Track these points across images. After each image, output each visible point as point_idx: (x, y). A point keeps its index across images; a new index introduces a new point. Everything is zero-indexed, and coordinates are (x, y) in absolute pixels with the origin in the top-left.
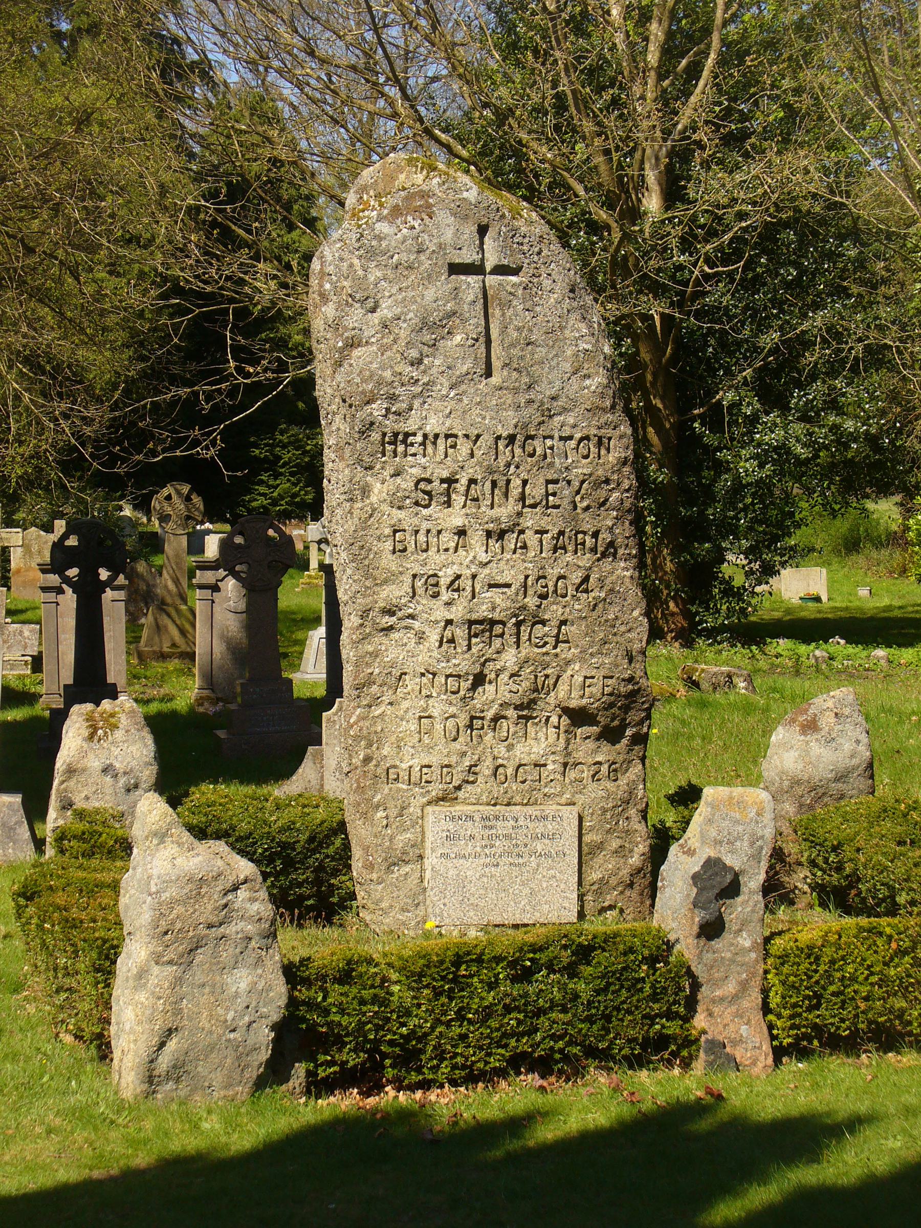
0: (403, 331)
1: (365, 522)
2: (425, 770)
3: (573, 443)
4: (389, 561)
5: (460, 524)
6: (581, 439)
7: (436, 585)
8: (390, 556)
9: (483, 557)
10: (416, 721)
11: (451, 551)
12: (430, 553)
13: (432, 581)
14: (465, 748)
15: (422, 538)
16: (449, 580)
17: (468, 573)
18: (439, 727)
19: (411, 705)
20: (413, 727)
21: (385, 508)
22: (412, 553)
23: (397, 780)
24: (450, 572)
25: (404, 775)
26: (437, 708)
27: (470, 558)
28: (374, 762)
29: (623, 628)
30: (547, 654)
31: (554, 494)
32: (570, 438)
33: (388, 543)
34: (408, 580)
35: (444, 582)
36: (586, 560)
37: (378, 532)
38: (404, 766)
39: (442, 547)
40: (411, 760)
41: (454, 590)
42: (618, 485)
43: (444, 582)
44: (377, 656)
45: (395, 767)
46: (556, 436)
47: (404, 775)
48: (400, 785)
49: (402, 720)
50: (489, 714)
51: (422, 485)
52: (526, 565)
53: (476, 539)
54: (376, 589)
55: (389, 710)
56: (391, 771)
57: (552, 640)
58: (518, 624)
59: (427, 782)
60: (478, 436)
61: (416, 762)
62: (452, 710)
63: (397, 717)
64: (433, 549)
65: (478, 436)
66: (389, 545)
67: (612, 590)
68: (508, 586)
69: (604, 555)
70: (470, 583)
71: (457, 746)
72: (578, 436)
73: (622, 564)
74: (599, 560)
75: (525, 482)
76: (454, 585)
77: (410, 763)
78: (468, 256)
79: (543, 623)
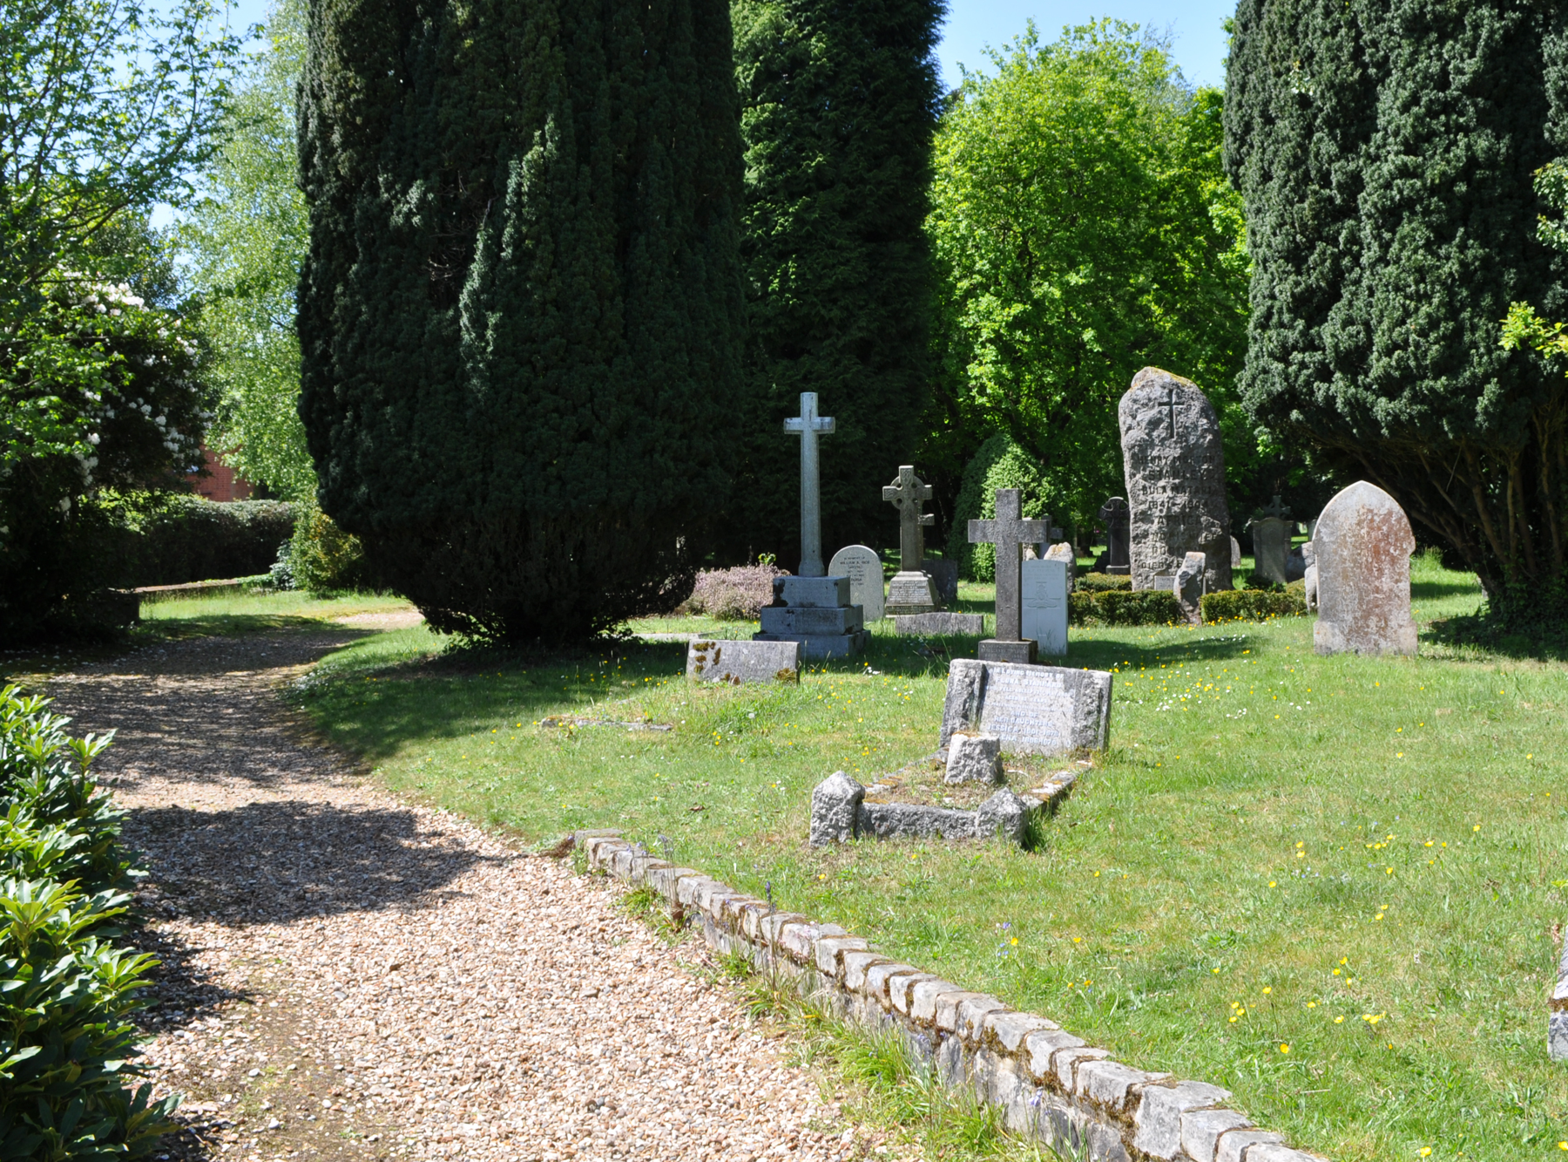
0: (1144, 425)
4: (1142, 498)
40: (1150, 561)
76: (1162, 504)
78: (1166, 400)
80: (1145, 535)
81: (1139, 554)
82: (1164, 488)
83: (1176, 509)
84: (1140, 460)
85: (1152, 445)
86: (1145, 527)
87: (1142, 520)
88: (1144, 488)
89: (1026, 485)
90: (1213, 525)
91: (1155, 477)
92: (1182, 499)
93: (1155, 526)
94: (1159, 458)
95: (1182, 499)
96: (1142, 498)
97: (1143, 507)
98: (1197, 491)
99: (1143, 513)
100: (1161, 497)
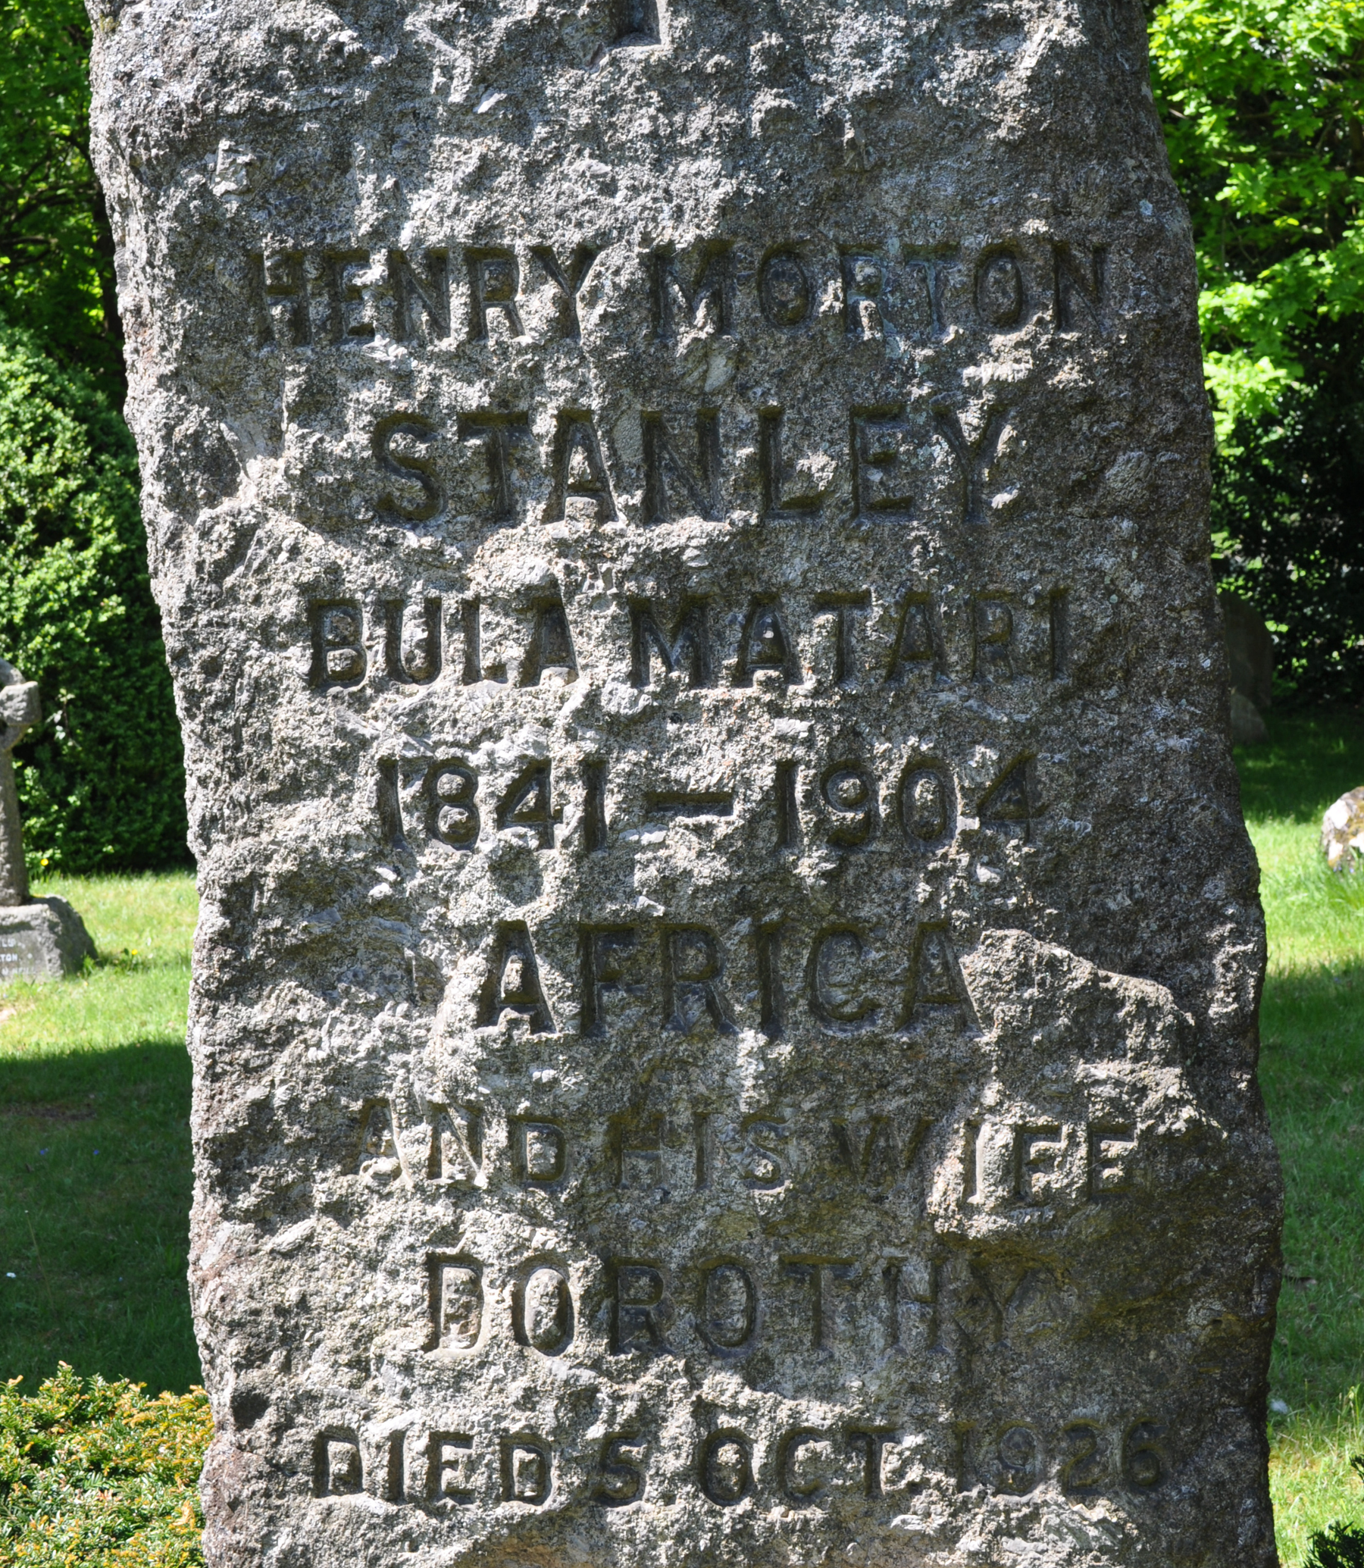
1: (218, 576)
2: (448, 1452)
3: (958, 275)
4: (300, 719)
5: (534, 578)
6: (993, 255)
7: (464, 797)
8: (302, 699)
9: (620, 698)
10: (419, 1274)
11: (513, 675)
12: (438, 685)
13: (447, 783)
14: (586, 1376)
15: (412, 632)
16: (504, 780)
17: (566, 754)
18: (495, 1301)
19: (399, 1215)
20: (411, 1289)
21: (284, 527)
22: (380, 686)
23: (352, 1481)
24: (507, 750)
25: (374, 1464)
26: (488, 1232)
27: (576, 701)
28: (270, 1416)
29: (1166, 946)
30: (878, 1044)
31: (886, 461)
32: (948, 251)
33: (294, 651)
34: (367, 783)
35: (489, 787)
36: (1014, 705)
37: (259, 613)
38: (376, 1431)
39: (486, 661)
41: (524, 819)
42: (1138, 417)
43: (489, 787)
44: (281, 1044)
45: (347, 1434)
46: (894, 245)
47: (374, 1464)
48: (361, 1500)
49: (372, 1265)
50: (679, 1251)
51: (398, 442)
52: (785, 725)
53: (592, 633)
54: (266, 811)
55: (327, 1230)
56: (334, 1447)
57: (892, 999)
58: (765, 938)
59: (454, 1492)
60: (585, 255)
61: (417, 1419)
62: (545, 1238)
63: (353, 1255)
64: (451, 671)
65: (585, 255)
66: (297, 659)
67: (1121, 809)
68: (718, 801)
69: (1086, 680)
70: (577, 793)
71: (556, 1368)
72: (976, 241)
73: (1162, 710)
74: (1065, 697)
75: (770, 420)
77: (398, 1423)
79: (856, 935)
80: (349, 1122)
81: (283, 1333)
82: (544, 611)
83: (680, 848)
84: (283, 296)
85: (400, 116)
86: (343, 1034)
87: (316, 965)
88: (324, 610)
89: (38, 485)
90: (1097, 1024)
91: (437, 480)
92: (736, 740)
93: (447, 1041)
94: (486, 262)
95: (736, 740)
96: (300, 719)
97: (310, 824)
98: (914, 650)
99: (315, 884)
100: (503, 716)
